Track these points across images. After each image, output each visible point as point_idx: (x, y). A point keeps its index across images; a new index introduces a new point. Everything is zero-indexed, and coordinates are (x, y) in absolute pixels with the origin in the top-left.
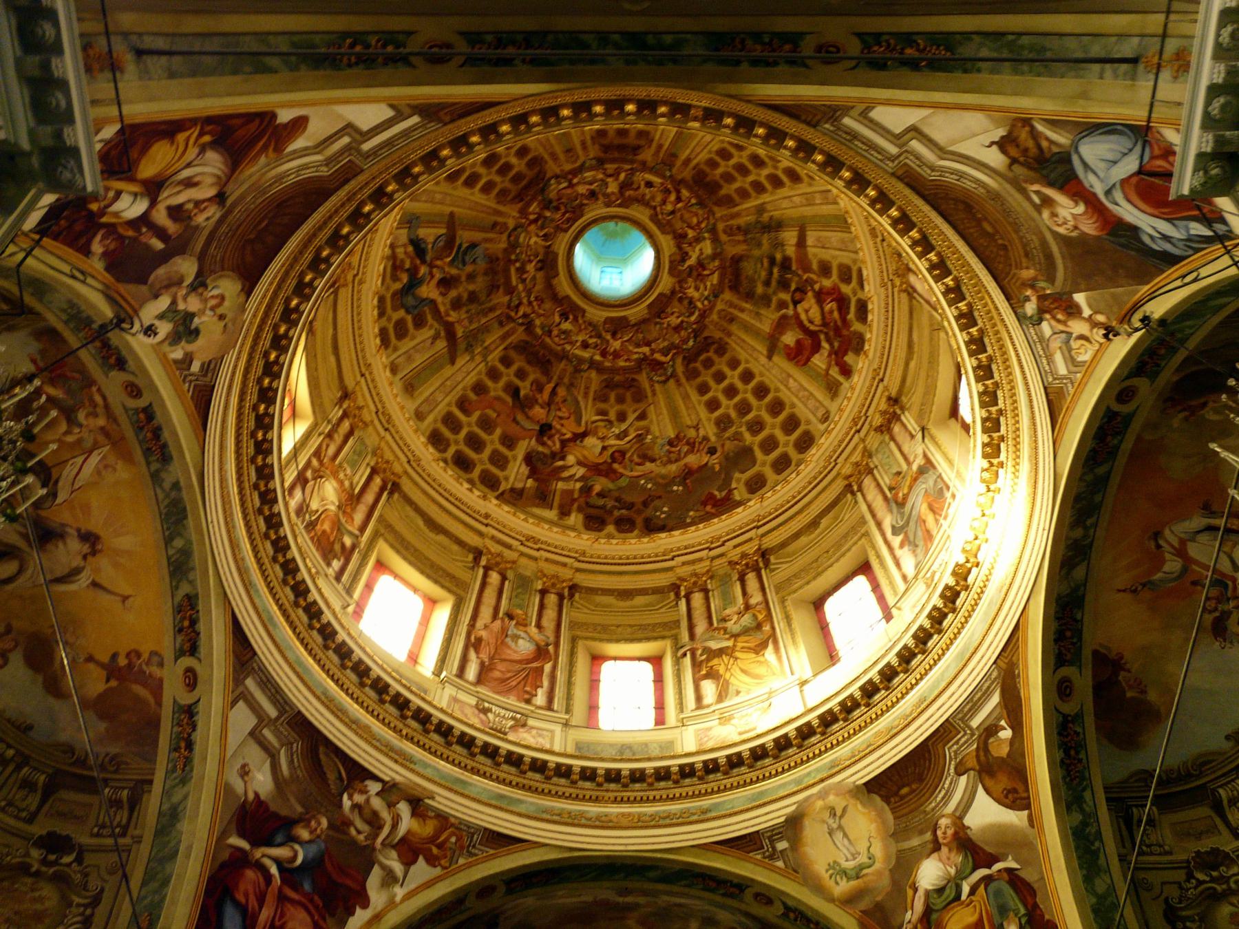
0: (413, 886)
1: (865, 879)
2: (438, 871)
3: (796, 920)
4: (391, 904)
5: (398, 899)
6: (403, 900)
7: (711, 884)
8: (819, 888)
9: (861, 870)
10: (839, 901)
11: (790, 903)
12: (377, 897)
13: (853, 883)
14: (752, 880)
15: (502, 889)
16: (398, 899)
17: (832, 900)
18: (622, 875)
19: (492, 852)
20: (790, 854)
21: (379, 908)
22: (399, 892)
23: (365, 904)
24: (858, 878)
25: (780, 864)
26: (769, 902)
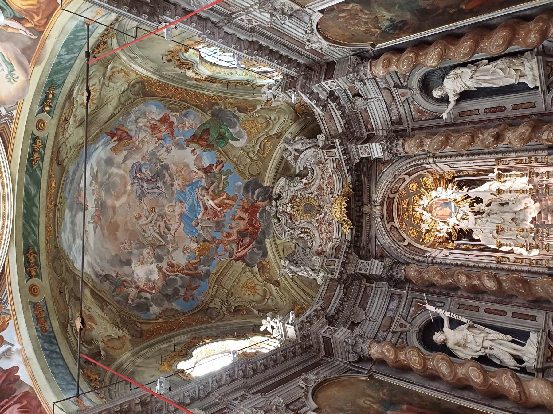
0: (15, 338)
1: (11, 59)
2: (11, 322)
3: (50, 106)
4: (21, 352)
5: (20, 347)
6: (22, 345)
7: (36, 155)
8: (24, 89)
9: (7, 61)
10: (28, 76)
11: (37, 109)
12: (15, 361)
13: (15, 66)
14: (26, 131)
15: (35, 281)
16: (20, 347)
17: (28, 81)
18: (34, 209)
19: (7, 288)
20: (7, 107)
21: (21, 359)
22: (17, 346)
23: (16, 369)
24: (11, 64)
25: (14, 113)
26: (41, 121)
